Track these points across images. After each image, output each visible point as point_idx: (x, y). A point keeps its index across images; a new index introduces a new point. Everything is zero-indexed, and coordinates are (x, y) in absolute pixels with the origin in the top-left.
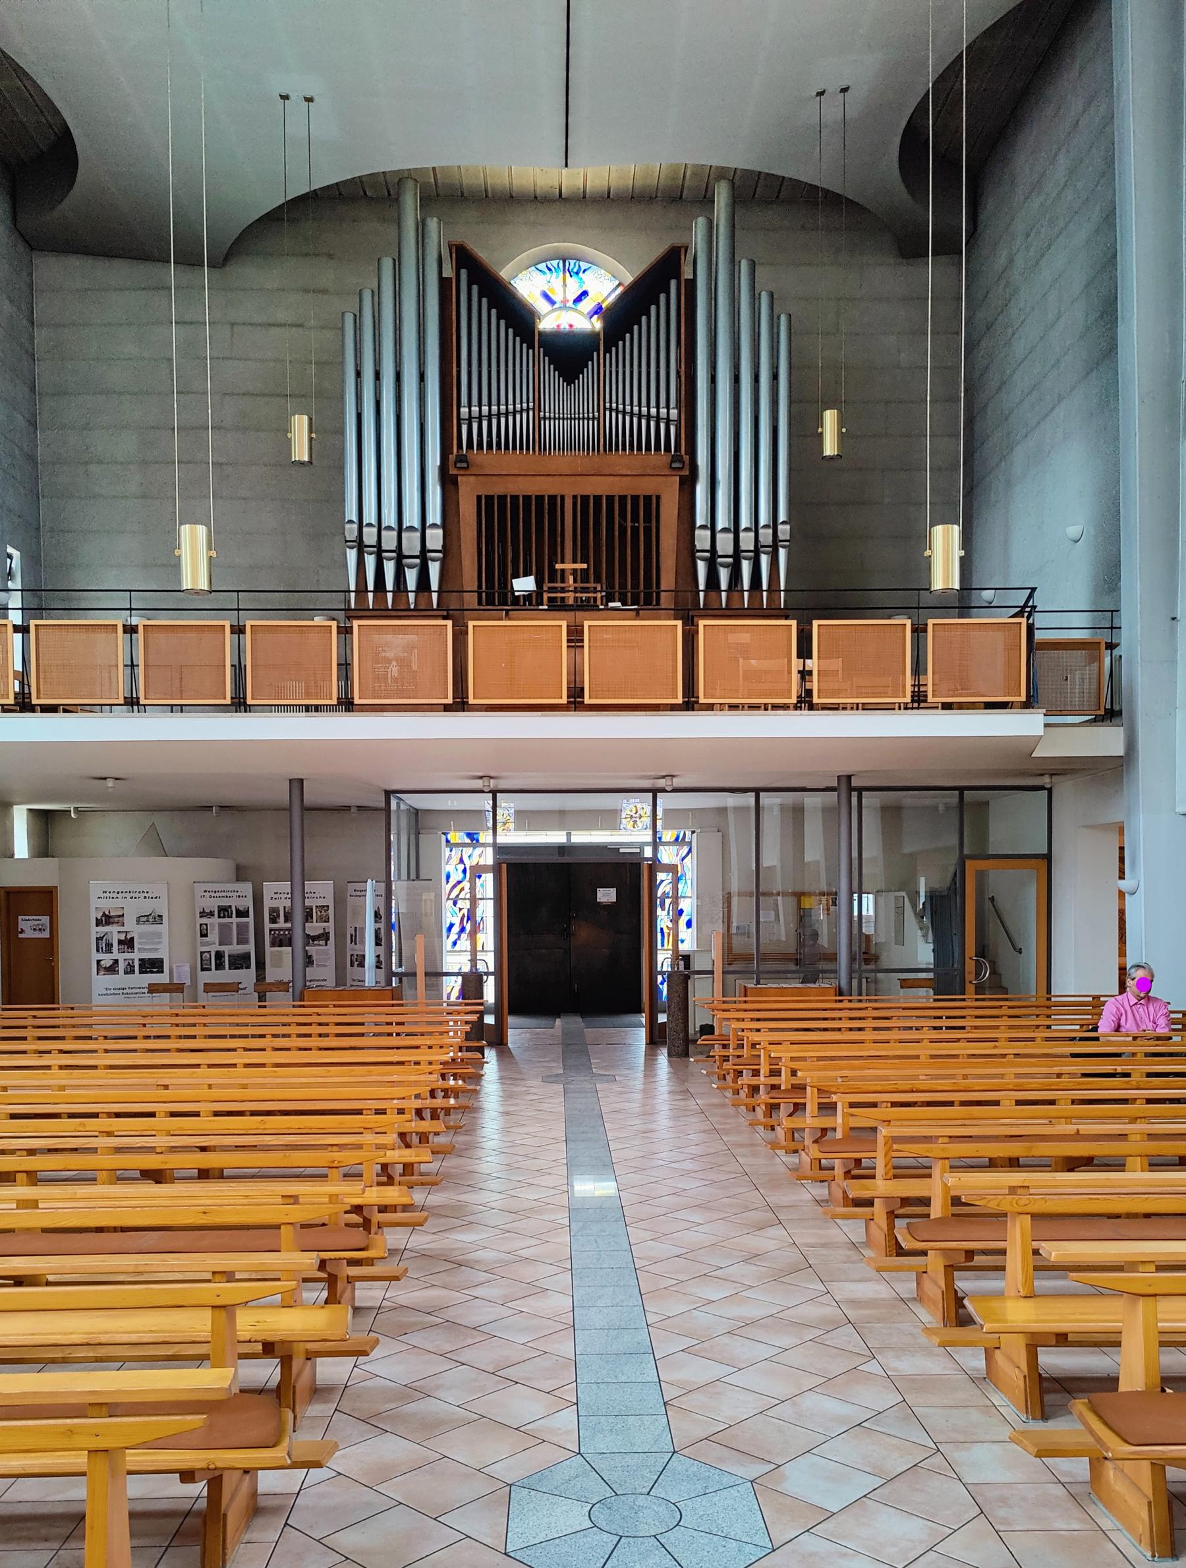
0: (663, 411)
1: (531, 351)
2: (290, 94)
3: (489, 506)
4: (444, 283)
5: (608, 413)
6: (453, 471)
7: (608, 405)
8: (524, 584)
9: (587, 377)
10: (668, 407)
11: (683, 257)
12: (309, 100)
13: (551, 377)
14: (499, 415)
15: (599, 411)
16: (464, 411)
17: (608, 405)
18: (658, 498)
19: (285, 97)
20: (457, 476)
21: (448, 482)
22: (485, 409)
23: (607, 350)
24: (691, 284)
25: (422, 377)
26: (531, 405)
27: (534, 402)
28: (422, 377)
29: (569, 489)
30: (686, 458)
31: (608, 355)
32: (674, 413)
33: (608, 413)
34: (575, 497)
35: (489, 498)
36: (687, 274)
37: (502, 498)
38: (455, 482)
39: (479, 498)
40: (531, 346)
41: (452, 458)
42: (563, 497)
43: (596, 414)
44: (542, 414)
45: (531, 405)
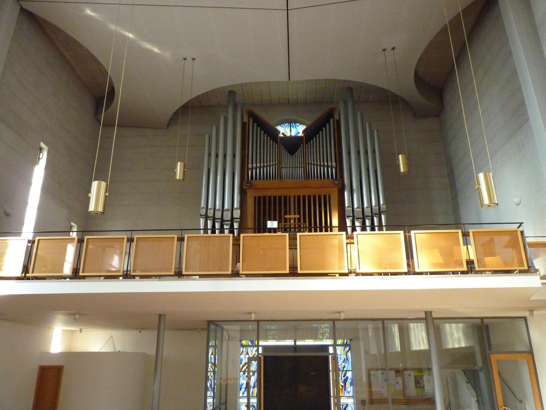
0: (330, 163)
1: (276, 145)
2: (187, 58)
3: (259, 201)
4: (244, 125)
5: (307, 165)
6: (245, 187)
7: (307, 162)
8: (272, 224)
9: (299, 153)
10: (332, 162)
11: (335, 111)
12: (194, 59)
13: (285, 153)
14: (264, 167)
15: (304, 164)
16: (250, 166)
17: (307, 162)
18: (329, 196)
19: (185, 59)
20: (246, 189)
21: (243, 193)
22: (258, 165)
23: (307, 143)
24: (338, 122)
25: (234, 156)
26: (277, 163)
27: (278, 162)
28: (234, 156)
29: (292, 193)
30: (340, 180)
31: (307, 145)
32: (334, 164)
33: (307, 165)
34: (295, 196)
35: (259, 197)
36: (336, 117)
37: (265, 197)
38: (246, 193)
39: (255, 197)
40: (277, 142)
41: (245, 182)
42: (290, 197)
43: (303, 165)
44: (281, 166)
45: (277, 163)
